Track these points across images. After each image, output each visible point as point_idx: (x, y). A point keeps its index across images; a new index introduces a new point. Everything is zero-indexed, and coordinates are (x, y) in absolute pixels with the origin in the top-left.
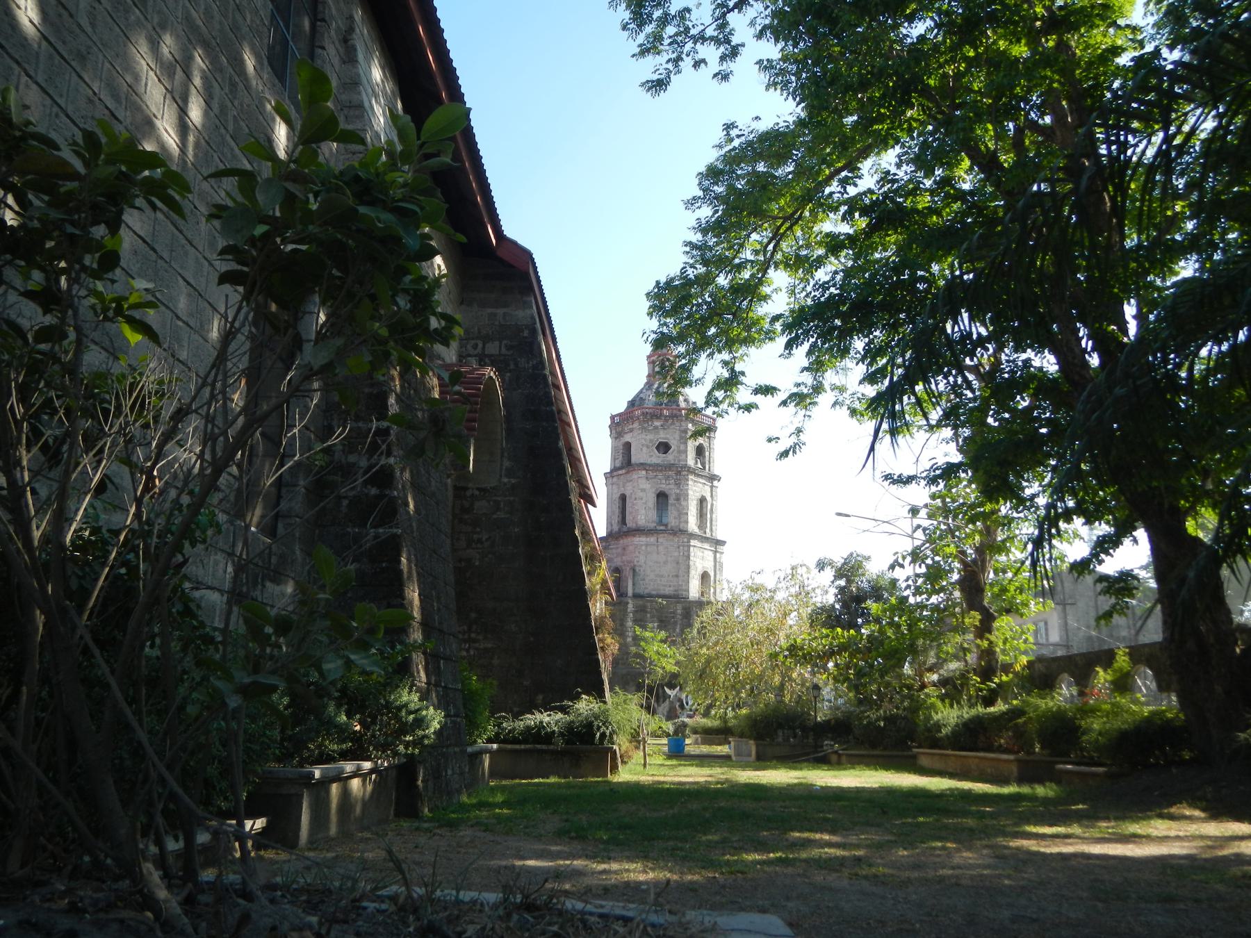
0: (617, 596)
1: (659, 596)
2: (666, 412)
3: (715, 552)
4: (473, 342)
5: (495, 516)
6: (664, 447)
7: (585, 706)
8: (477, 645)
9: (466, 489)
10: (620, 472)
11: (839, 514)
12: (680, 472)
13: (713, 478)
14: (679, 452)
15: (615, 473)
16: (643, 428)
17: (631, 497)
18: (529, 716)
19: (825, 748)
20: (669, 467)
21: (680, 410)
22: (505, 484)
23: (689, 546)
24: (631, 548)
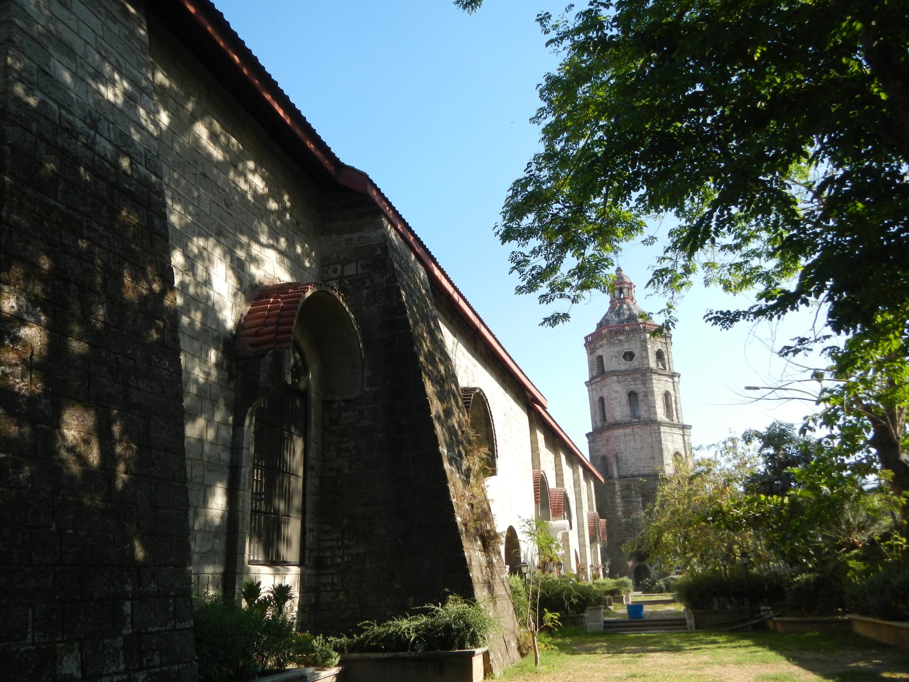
0: (605, 479)
2: (627, 328)
3: (683, 435)
5: (360, 425)
6: (629, 356)
7: (453, 607)
10: (597, 380)
11: (748, 388)
12: (645, 374)
13: (673, 375)
14: (642, 358)
15: (593, 381)
16: (610, 343)
17: (607, 399)
18: (390, 622)
19: (762, 613)
20: (636, 370)
21: (639, 325)
23: (660, 433)
24: (612, 439)
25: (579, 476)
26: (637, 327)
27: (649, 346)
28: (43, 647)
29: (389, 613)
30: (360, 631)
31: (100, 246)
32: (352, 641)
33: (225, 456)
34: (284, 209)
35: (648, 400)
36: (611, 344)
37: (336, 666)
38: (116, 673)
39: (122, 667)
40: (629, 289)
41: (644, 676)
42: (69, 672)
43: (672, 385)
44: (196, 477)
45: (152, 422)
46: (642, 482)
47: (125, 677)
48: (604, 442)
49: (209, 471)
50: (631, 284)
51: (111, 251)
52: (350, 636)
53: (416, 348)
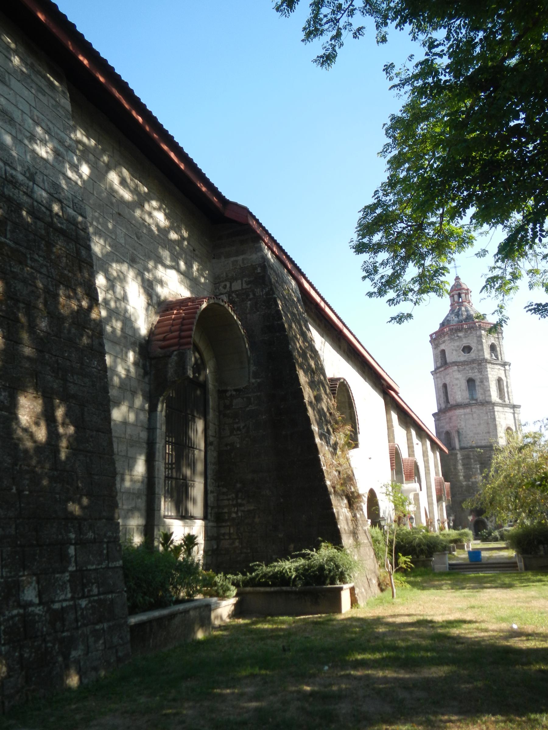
1: (477, 447)
3: (514, 413)
4: (223, 284)
5: (248, 409)
6: (467, 349)
8: (243, 508)
9: (226, 391)
10: (441, 369)
13: (504, 364)
14: (478, 351)
15: (438, 371)
18: (276, 564)
20: (473, 361)
22: (253, 384)
23: (494, 412)
24: (454, 418)
25: (427, 448)
26: (474, 325)
27: (484, 341)
28: (10, 580)
29: (274, 557)
30: (252, 570)
31: (41, 273)
32: (246, 578)
33: (144, 435)
34: (183, 238)
35: (484, 385)
36: (452, 340)
37: (234, 597)
38: (65, 600)
39: (69, 595)
40: (467, 294)
41: (481, 607)
42: (29, 599)
43: (503, 372)
44: (121, 451)
45: (86, 409)
46: (479, 452)
47: (71, 603)
48: (447, 420)
49: (132, 446)
50: (468, 290)
51: (49, 277)
52: (244, 574)
53: (290, 347)
